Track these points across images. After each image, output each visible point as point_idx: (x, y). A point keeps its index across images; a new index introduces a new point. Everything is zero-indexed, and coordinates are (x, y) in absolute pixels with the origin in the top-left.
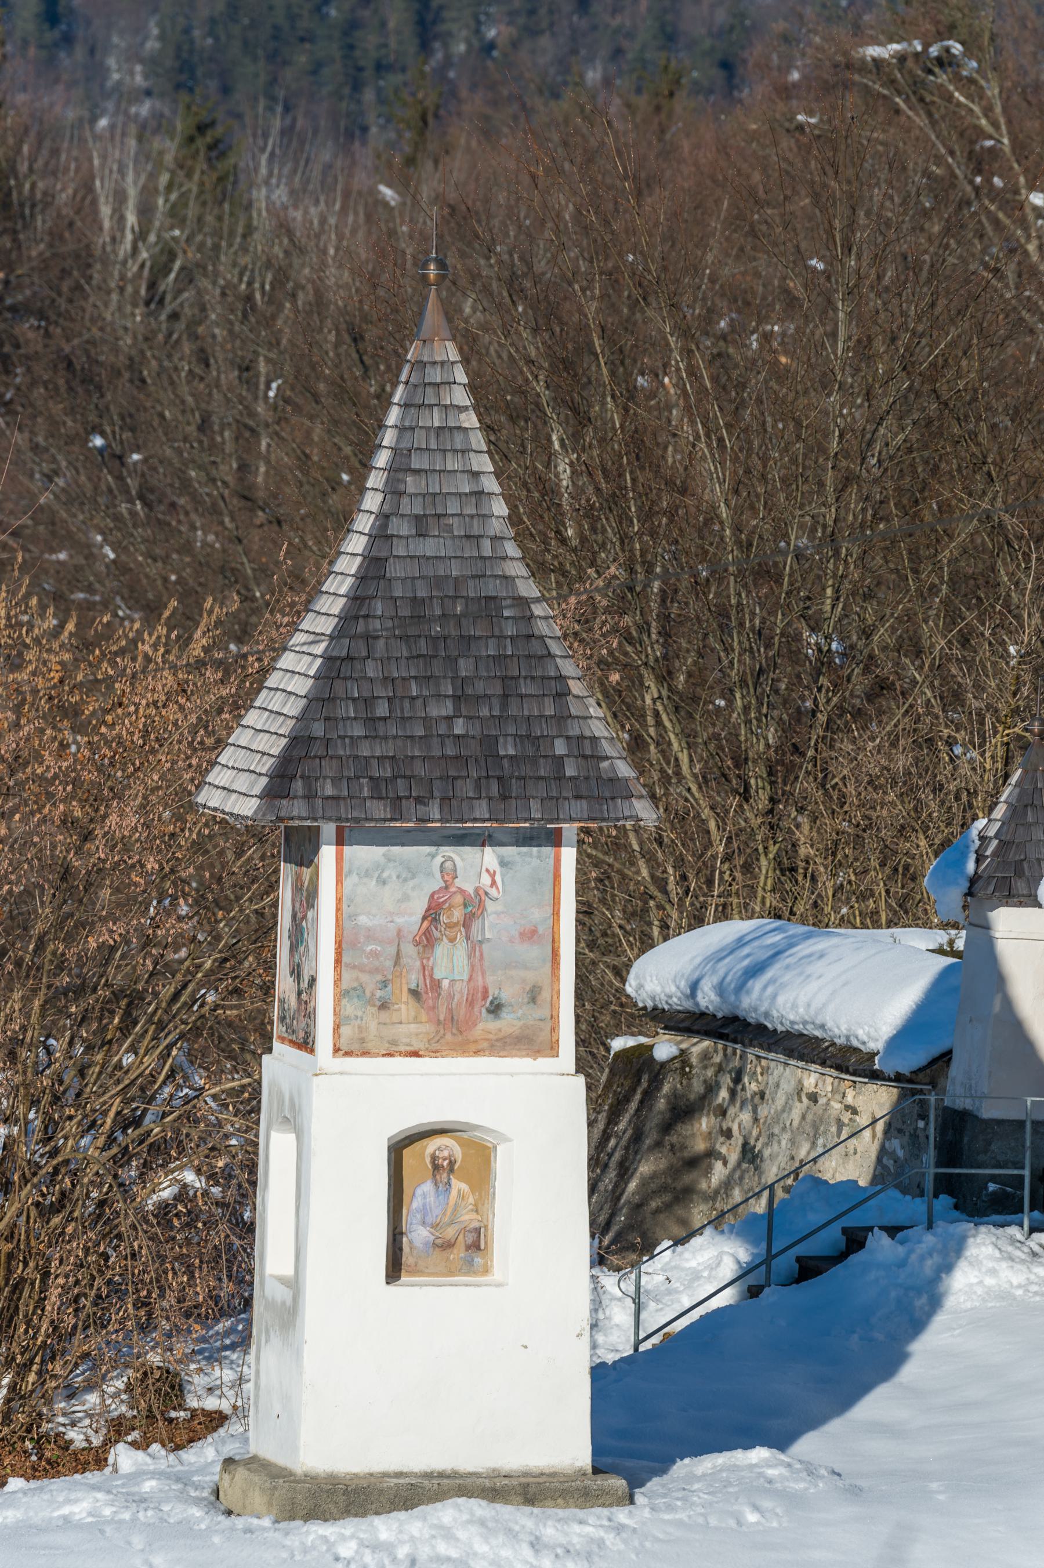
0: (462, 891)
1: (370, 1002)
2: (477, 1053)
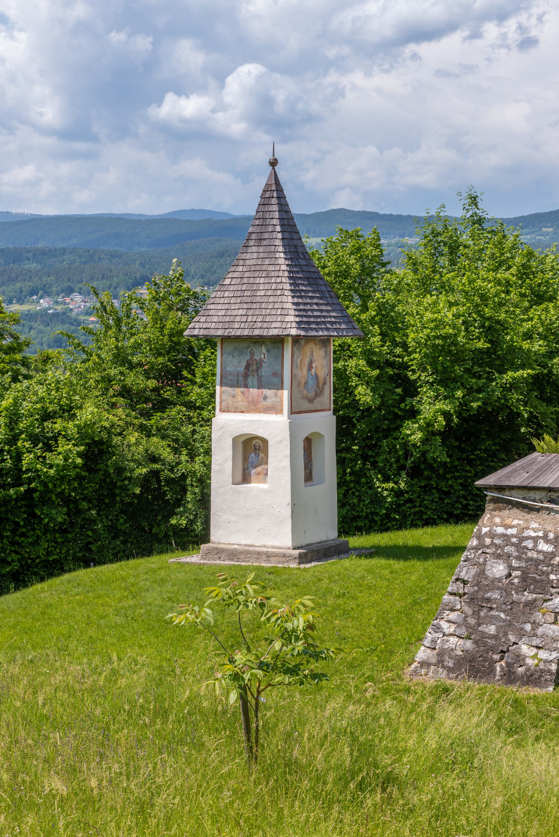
0: (256, 360)
1: (230, 395)
2: (260, 412)
